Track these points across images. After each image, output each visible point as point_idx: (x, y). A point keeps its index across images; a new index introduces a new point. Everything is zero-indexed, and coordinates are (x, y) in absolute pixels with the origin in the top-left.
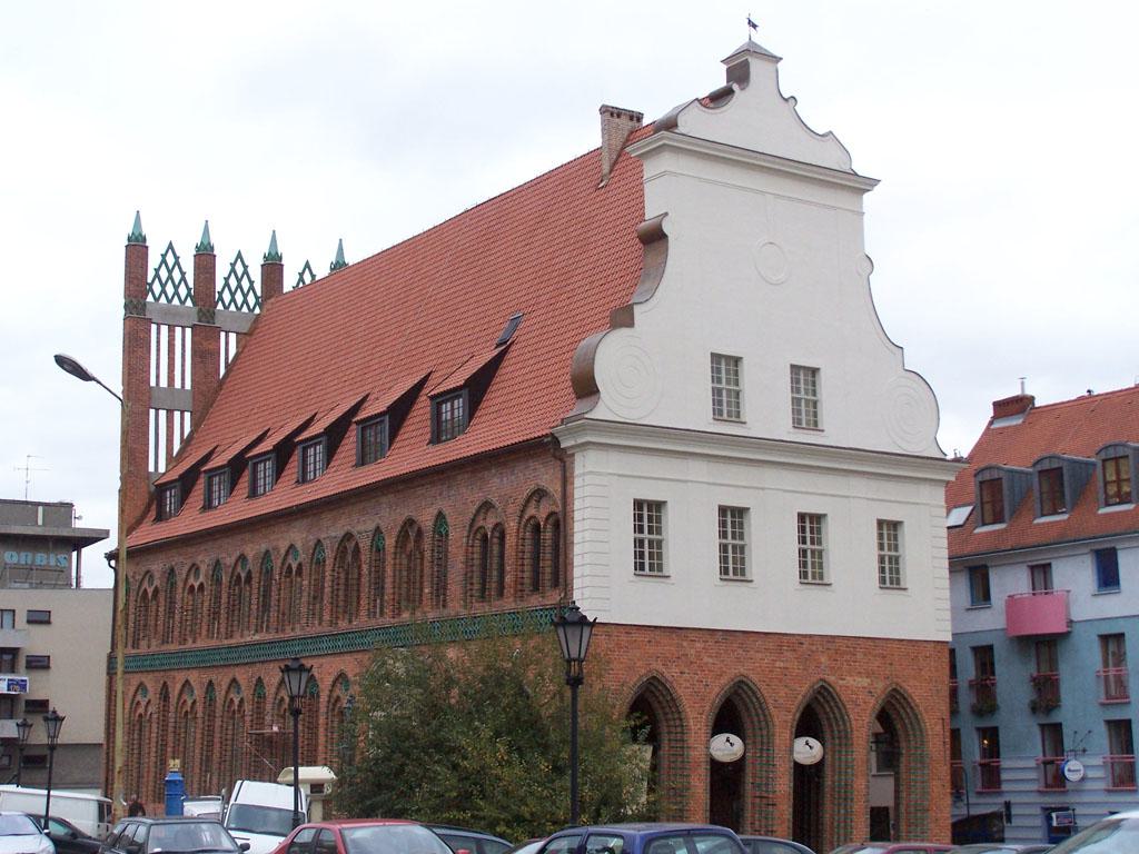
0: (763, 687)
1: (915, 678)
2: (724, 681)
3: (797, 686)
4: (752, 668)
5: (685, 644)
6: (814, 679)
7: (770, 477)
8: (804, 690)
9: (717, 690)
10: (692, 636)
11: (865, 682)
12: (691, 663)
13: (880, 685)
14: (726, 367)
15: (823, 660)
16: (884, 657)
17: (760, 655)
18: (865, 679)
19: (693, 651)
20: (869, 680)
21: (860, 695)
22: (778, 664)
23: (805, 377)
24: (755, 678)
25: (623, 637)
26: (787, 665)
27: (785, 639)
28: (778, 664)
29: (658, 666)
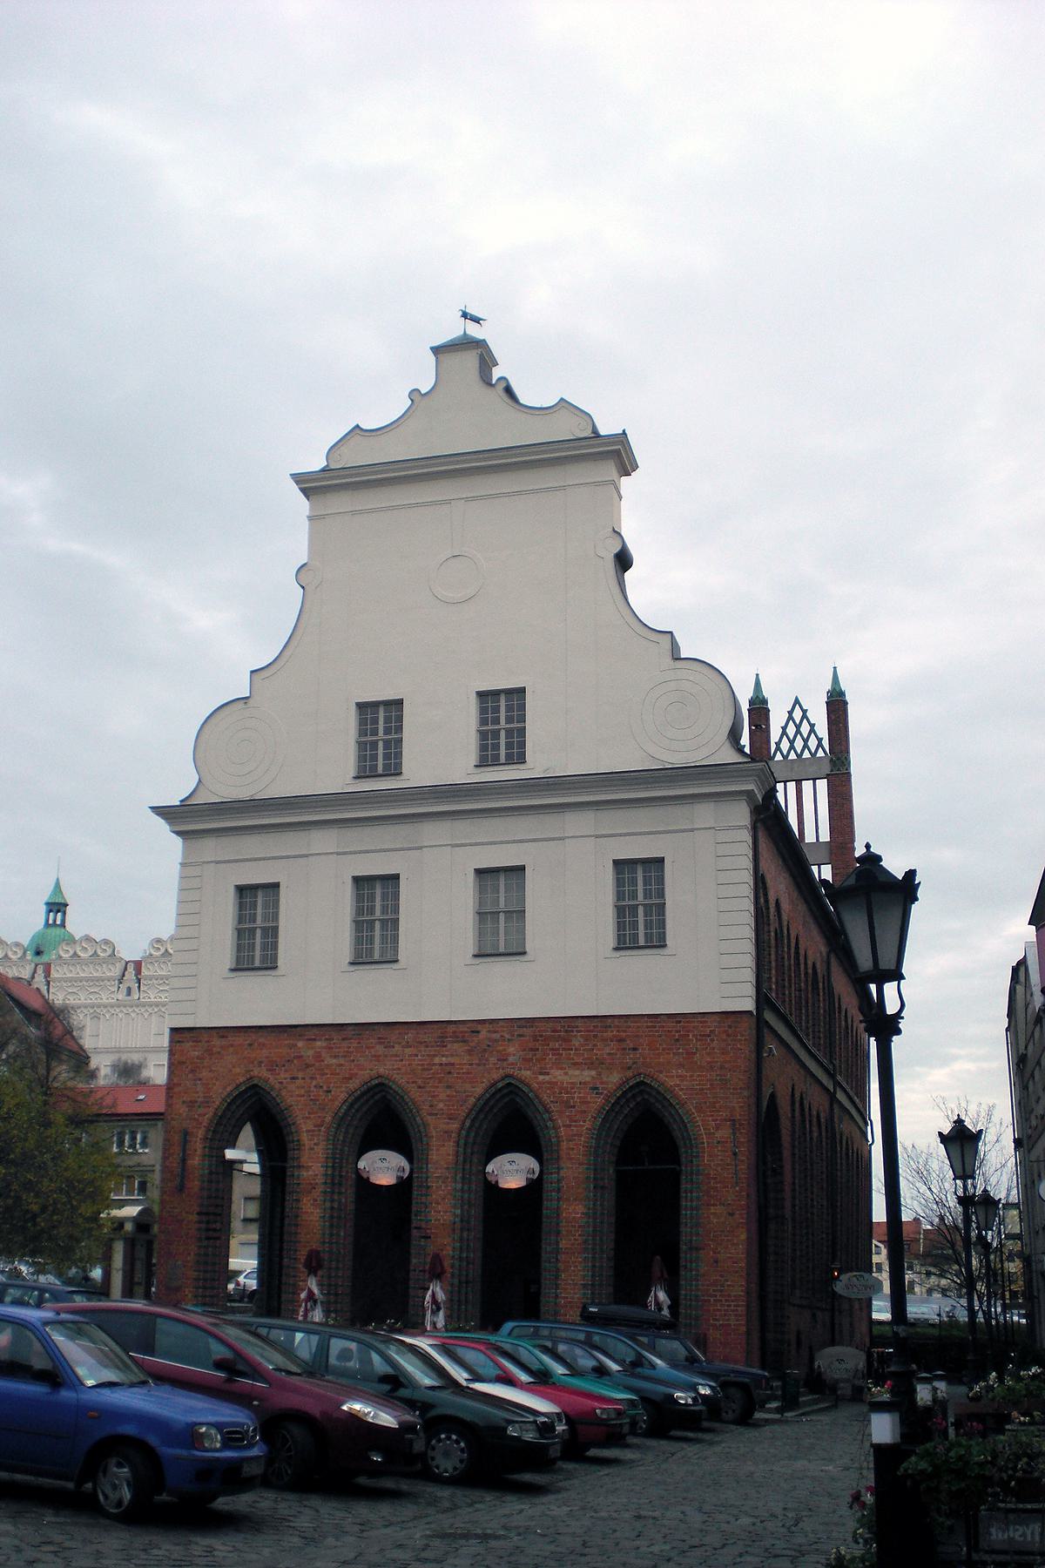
0: (414, 1093)
1: (681, 1065)
2: (354, 1084)
3: (468, 1086)
4: (394, 1067)
5: (300, 1044)
6: (496, 1076)
7: (433, 832)
8: (479, 1090)
9: (343, 1096)
10: (310, 1034)
11: (587, 1075)
12: (308, 1066)
13: (614, 1079)
14: (380, 723)
15: (511, 1050)
16: (621, 1040)
17: (408, 1051)
18: (586, 1073)
19: (310, 1053)
20: (593, 1073)
21: (575, 1096)
22: (437, 1060)
23: (502, 717)
24: (402, 1080)
25: (217, 1042)
26: (451, 1060)
27: (451, 1028)
28: (437, 1060)
29: (261, 1072)
